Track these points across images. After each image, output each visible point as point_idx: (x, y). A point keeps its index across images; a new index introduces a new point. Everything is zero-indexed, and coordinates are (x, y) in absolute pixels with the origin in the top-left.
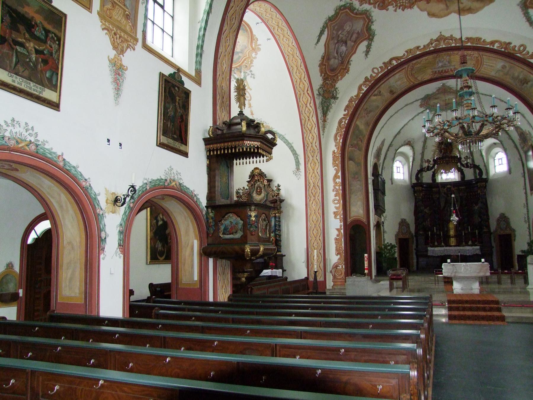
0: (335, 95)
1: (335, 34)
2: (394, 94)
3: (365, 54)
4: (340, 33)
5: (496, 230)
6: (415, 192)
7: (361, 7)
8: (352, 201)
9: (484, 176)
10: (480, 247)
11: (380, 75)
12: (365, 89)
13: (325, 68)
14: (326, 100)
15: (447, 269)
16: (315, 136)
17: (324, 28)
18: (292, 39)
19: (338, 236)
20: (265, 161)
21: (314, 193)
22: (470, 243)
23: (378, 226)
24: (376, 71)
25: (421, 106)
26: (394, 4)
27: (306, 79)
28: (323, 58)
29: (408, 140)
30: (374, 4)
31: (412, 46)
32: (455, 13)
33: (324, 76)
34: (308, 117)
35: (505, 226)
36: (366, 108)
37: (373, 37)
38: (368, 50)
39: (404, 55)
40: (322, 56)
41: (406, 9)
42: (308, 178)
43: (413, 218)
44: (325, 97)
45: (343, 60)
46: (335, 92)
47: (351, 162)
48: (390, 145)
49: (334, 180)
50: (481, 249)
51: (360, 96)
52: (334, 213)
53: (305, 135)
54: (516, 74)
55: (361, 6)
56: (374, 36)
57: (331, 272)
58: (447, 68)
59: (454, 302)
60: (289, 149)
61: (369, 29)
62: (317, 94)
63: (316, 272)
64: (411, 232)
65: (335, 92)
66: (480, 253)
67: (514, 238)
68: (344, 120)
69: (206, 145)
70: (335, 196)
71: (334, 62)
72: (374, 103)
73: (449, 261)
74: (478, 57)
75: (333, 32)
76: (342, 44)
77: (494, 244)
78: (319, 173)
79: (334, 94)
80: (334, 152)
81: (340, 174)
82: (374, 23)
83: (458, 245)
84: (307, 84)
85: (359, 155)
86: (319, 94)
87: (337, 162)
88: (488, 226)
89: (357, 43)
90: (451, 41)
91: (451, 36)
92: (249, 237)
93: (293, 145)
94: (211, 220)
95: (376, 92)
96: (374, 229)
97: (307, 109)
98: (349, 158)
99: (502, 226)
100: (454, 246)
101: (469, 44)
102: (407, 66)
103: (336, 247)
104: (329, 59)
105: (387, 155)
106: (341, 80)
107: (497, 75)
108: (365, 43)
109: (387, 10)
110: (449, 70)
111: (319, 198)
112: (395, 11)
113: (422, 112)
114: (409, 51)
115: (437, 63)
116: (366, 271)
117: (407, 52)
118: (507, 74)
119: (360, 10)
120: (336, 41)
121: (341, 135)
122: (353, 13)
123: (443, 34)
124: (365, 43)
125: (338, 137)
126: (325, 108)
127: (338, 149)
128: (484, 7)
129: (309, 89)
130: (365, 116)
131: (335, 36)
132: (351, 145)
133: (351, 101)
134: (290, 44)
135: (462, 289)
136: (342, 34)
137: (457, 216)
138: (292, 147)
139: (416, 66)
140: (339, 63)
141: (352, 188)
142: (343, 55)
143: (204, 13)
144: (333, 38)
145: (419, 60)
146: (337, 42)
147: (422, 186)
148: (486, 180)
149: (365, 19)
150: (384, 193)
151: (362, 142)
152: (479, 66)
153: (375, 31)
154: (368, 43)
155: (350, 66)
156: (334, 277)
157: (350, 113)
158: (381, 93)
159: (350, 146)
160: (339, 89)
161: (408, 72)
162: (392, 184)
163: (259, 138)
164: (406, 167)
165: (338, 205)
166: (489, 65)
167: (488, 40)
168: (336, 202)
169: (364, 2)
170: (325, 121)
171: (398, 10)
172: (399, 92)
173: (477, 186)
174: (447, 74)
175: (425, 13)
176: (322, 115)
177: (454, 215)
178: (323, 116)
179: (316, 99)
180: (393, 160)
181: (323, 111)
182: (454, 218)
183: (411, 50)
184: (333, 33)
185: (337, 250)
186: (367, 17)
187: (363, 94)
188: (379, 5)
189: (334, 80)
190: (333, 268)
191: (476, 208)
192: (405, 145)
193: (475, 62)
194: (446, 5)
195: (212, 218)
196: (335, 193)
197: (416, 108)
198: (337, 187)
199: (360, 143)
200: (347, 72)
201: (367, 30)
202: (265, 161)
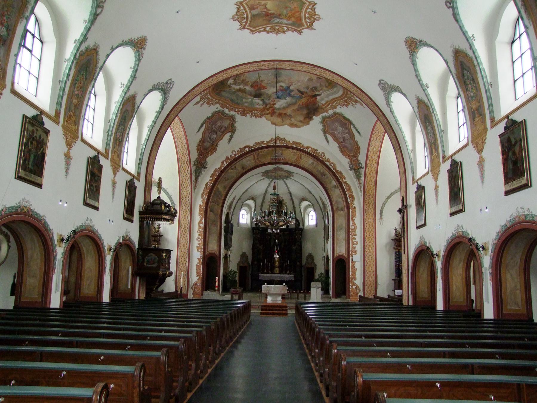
4: (214, 126)
5: (306, 264)
6: (254, 234)
7: (229, 113)
8: (210, 240)
9: (301, 226)
10: (294, 275)
11: (237, 156)
12: (226, 164)
15: (265, 288)
16: (188, 193)
17: (204, 123)
18: (182, 129)
19: (198, 263)
20: (169, 224)
21: (184, 233)
22: (288, 272)
23: (226, 257)
24: (234, 153)
25: (263, 176)
27: (187, 154)
28: (200, 141)
29: (253, 196)
30: (238, 112)
31: (259, 141)
34: (185, 179)
37: (235, 131)
39: (254, 145)
42: (181, 222)
43: (251, 252)
47: (211, 213)
48: (239, 199)
49: (199, 224)
50: (295, 277)
52: (197, 247)
53: (181, 191)
55: (229, 112)
57: (192, 288)
59: (265, 306)
60: (169, 199)
63: (182, 287)
64: (248, 262)
66: (293, 280)
69: (139, 214)
70: (199, 236)
71: (207, 144)
73: (266, 284)
77: (303, 274)
78: (189, 219)
80: (200, 205)
81: (203, 221)
83: (281, 272)
84: (187, 158)
85: (217, 208)
86: (195, 165)
87: (202, 212)
88: (301, 261)
89: (224, 133)
91: (284, 138)
92: (161, 266)
93: (172, 197)
94: (140, 256)
95: (233, 167)
96: (223, 259)
97: (185, 174)
100: (278, 274)
101: (294, 146)
103: (197, 271)
104: (204, 142)
105: (237, 206)
107: (309, 167)
108: (229, 134)
111: (187, 236)
113: (263, 179)
114: (257, 143)
116: (216, 288)
117: (255, 143)
118: (315, 168)
120: (210, 132)
121: (206, 194)
122: (223, 116)
123: (279, 136)
124: (229, 134)
127: (203, 203)
128: (303, 126)
129: (188, 161)
133: (215, 171)
134: (180, 132)
135: (272, 300)
137: (278, 255)
138: (171, 198)
143: (145, 140)
145: (263, 150)
146: (211, 132)
147: (259, 230)
148: (302, 230)
150: (232, 234)
151: (220, 199)
152: (299, 160)
156: (194, 292)
157: (214, 179)
160: (208, 162)
162: (238, 226)
163: (171, 215)
164: (249, 215)
165: (200, 242)
166: (305, 161)
167: (305, 146)
168: (199, 240)
170: (196, 183)
173: (296, 233)
174: (279, 161)
175: (270, 122)
177: (276, 254)
180: (240, 209)
181: (196, 176)
182: (276, 256)
183: (258, 142)
185: (197, 273)
186: (233, 119)
187: (224, 167)
188: (241, 113)
189: (205, 155)
190: (194, 285)
191: (294, 248)
192: (249, 199)
194: (282, 120)
195: (141, 255)
196: (199, 233)
197: (260, 177)
198: (201, 230)
200: (215, 151)
201: (231, 127)
202: (169, 224)
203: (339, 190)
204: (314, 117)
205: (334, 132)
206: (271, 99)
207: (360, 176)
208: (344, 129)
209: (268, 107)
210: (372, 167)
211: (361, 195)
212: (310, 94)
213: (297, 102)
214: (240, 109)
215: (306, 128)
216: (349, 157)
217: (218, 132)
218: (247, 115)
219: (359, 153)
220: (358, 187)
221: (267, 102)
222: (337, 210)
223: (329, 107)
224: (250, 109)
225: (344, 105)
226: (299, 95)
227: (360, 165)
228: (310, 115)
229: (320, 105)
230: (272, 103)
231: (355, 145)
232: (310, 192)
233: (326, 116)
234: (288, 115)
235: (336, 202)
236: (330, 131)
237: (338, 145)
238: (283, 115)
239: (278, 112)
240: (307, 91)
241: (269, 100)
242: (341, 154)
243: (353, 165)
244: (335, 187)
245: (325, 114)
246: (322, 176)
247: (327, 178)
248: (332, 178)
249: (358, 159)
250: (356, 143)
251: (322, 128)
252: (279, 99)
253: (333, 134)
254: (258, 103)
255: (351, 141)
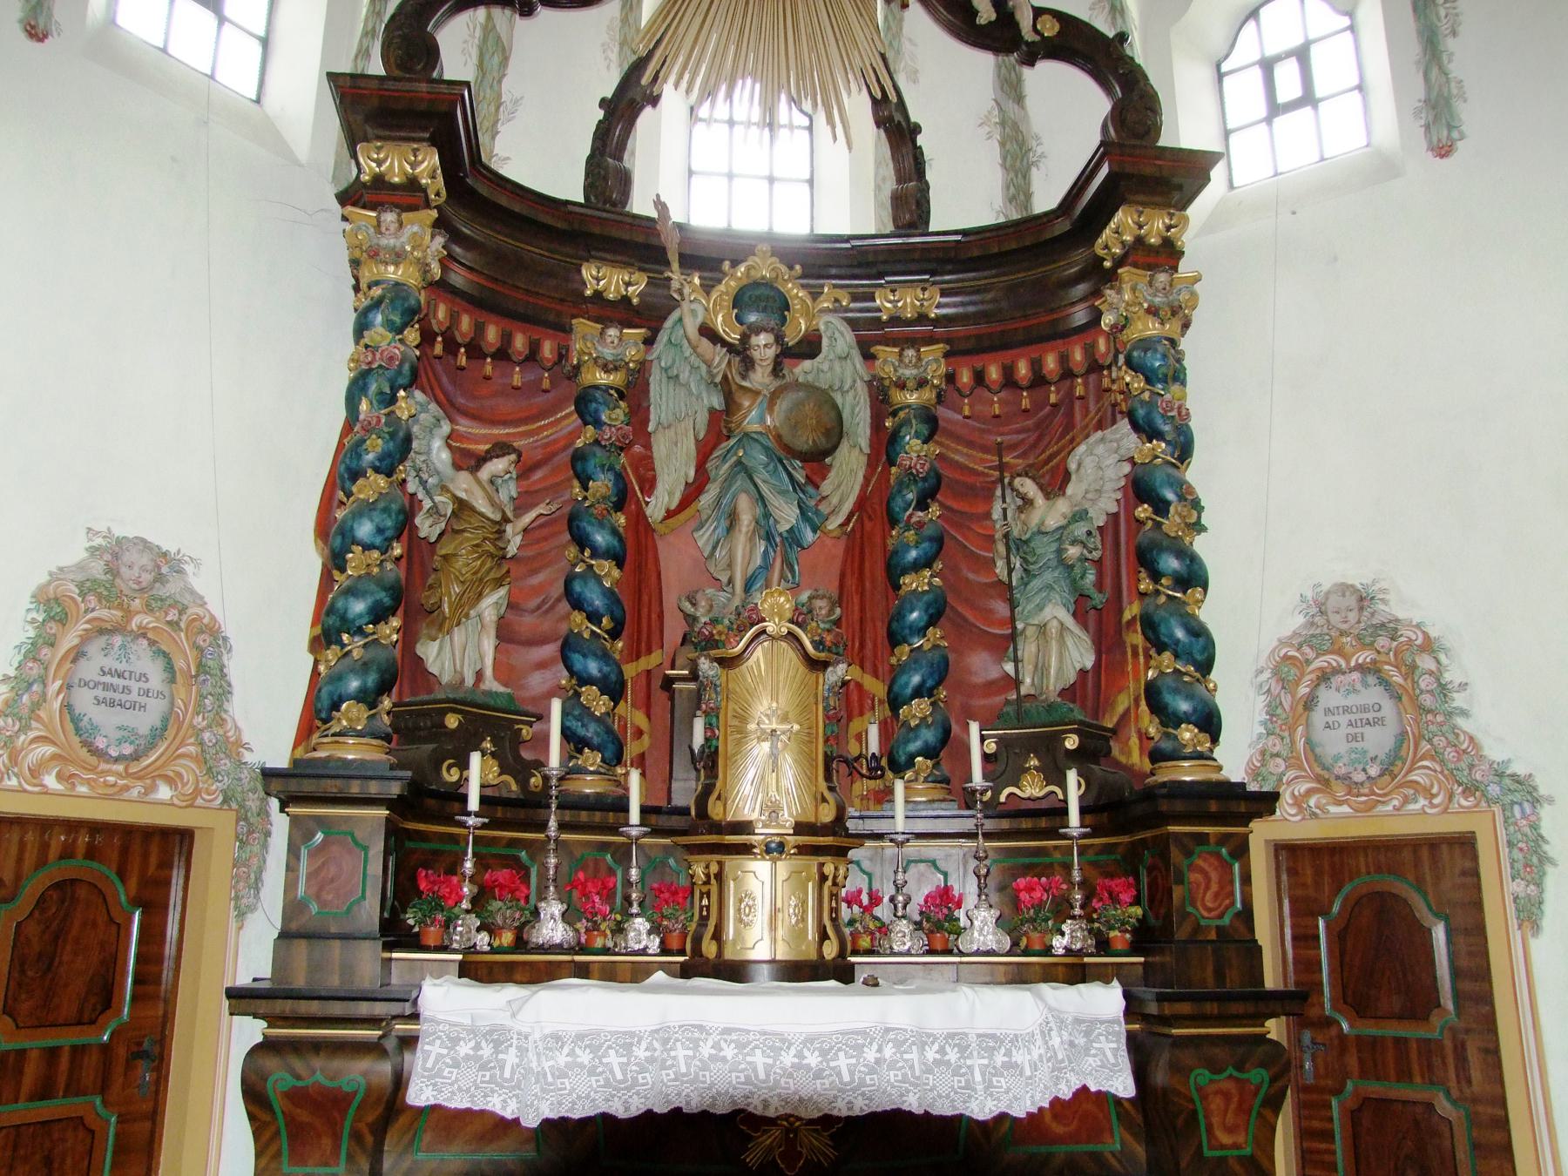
35: (1379, 741)
66: (1123, 1085)
67: (1517, 887)
99: (1334, 744)
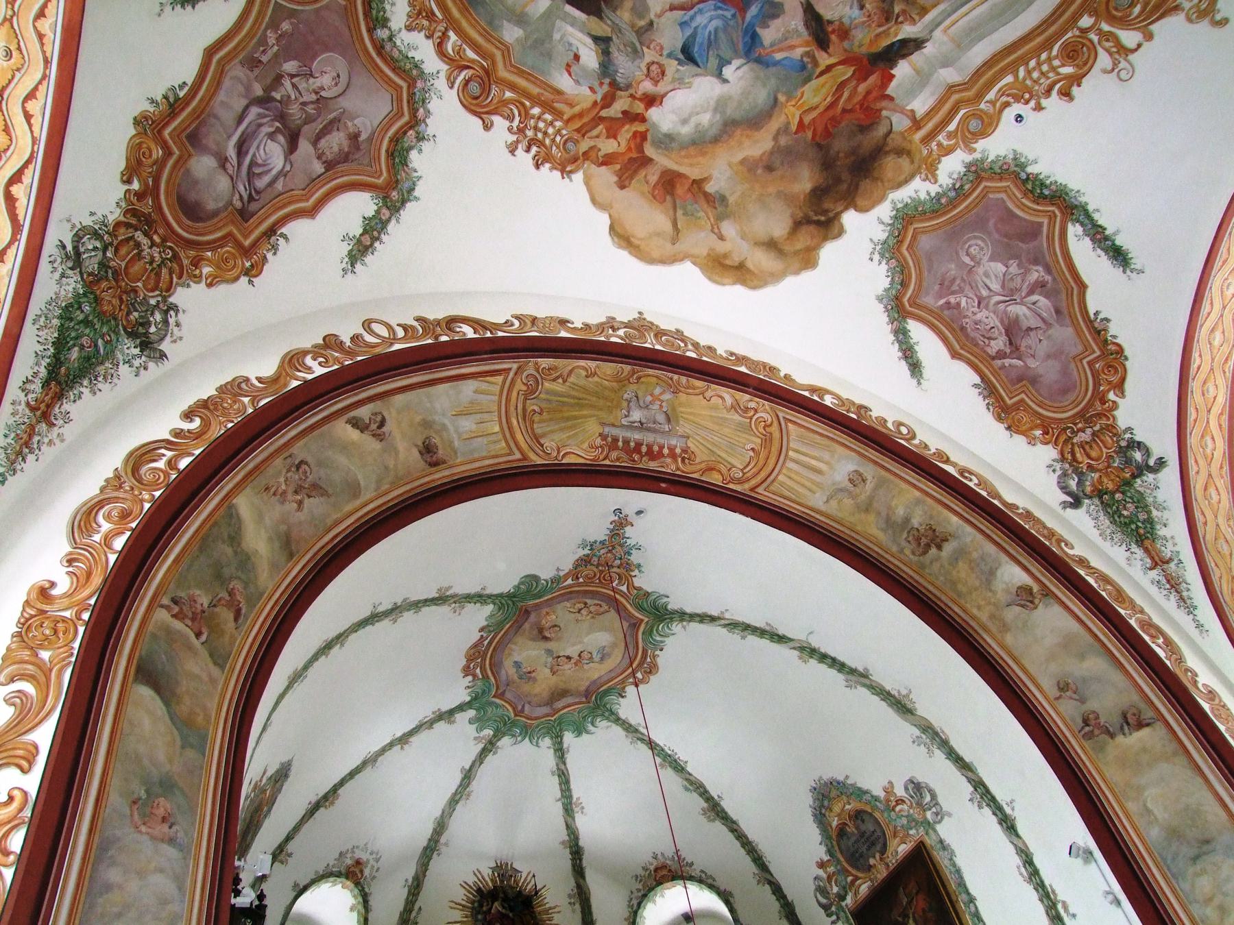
0: (153, 329)
1: (270, 53)
2: (434, 464)
3: (350, 252)
4: (290, 66)
11: (397, 347)
13: (161, 164)
14: (101, 315)
26: (517, 119)
29: (360, 854)
30: (456, 64)
32: (694, 263)
33: (140, 196)
36: (302, 462)
37: (404, 202)
38: (367, 240)
40: (173, 89)
41: (547, 165)
44: (97, 300)
45: (253, 206)
46: (158, 316)
51: (286, 385)
54: (901, 512)
55: (409, 28)
56: (409, 200)
58: (660, 440)
61: (398, 155)
62: (64, 247)
65: (158, 316)
68: (169, 454)
72: (342, 460)
74: (771, 425)
75: (264, 38)
76: (278, 130)
79: (148, 324)
81: (44, 736)
82: (425, 146)
87: (45, 655)
90: (682, 345)
95: (364, 412)
98: (139, 670)
102: (515, 366)
106: (210, 285)
107: (832, 508)
109: (487, 127)
110: (666, 451)
112: (512, 150)
115: (625, 404)
118: (867, 508)
119: (398, 43)
120: (258, 91)
121: (125, 515)
122: (371, 31)
125: (100, 519)
126: (75, 354)
129: (32, 177)
130: (284, 492)
131: (265, 59)
132: (175, 601)
136: (294, 86)
139: (547, 384)
140: (230, 203)
141: (113, 875)
142: (261, 183)
144: (253, 63)
149: (400, 100)
151: (236, 619)
153: (419, 178)
154: (378, 212)
155: (269, 256)
157: (216, 431)
158: (384, 429)
159: (166, 601)
161: (514, 394)
169: (426, 23)
171: (520, 151)
172: (461, 466)
174: (653, 465)
175: (603, 220)
176: (43, 372)
178: (46, 384)
179: (44, 267)
181: (53, 370)
184: (263, 41)
188: (467, 82)
189: (176, 257)
192: (338, 875)
193: (759, 441)
199: (227, 615)
201: (391, 155)
203: (1057, 609)
204: (850, 218)
205: (952, 300)
206: (649, 55)
207: (1150, 521)
208: (1014, 269)
209: (616, 110)
210: (1208, 451)
211: (1199, 626)
212: (864, 40)
213: (776, 100)
214: (470, 54)
215: (795, 286)
216: (1051, 432)
217: (304, 146)
218: (497, 119)
219: (1120, 387)
220: (1153, 590)
221: (625, 66)
222: (1089, 736)
223: (950, 136)
224: (522, 82)
225: (1048, 92)
226: (798, 53)
227: (1138, 456)
228: (827, 205)
229: (900, 123)
230: (647, 86)
231: (1086, 347)
232: (715, 810)
233: (917, 203)
234: (707, 195)
235: (1063, 687)
236: (929, 300)
237: (977, 380)
238: (680, 190)
239: (663, 161)
240: (856, 12)
241: (636, 54)
242: (1000, 428)
243: (1081, 475)
244: (1025, 597)
245: (918, 189)
246: (925, 553)
247: (960, 553)
248: (990, 548)
249: (1111, 428)
250: (1097, 330)
251: (886, 283)
252: (688, 69)
253: (946, 312)
254: (577, 57)
255: (1063, 334)
